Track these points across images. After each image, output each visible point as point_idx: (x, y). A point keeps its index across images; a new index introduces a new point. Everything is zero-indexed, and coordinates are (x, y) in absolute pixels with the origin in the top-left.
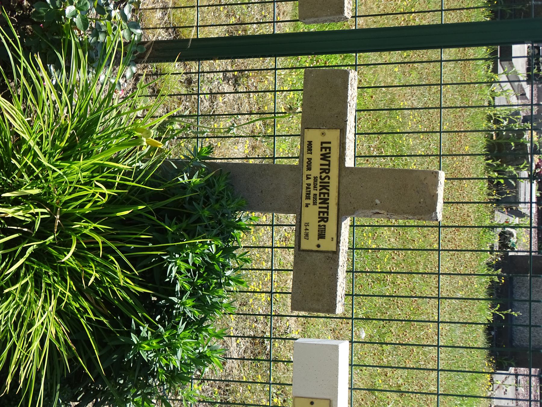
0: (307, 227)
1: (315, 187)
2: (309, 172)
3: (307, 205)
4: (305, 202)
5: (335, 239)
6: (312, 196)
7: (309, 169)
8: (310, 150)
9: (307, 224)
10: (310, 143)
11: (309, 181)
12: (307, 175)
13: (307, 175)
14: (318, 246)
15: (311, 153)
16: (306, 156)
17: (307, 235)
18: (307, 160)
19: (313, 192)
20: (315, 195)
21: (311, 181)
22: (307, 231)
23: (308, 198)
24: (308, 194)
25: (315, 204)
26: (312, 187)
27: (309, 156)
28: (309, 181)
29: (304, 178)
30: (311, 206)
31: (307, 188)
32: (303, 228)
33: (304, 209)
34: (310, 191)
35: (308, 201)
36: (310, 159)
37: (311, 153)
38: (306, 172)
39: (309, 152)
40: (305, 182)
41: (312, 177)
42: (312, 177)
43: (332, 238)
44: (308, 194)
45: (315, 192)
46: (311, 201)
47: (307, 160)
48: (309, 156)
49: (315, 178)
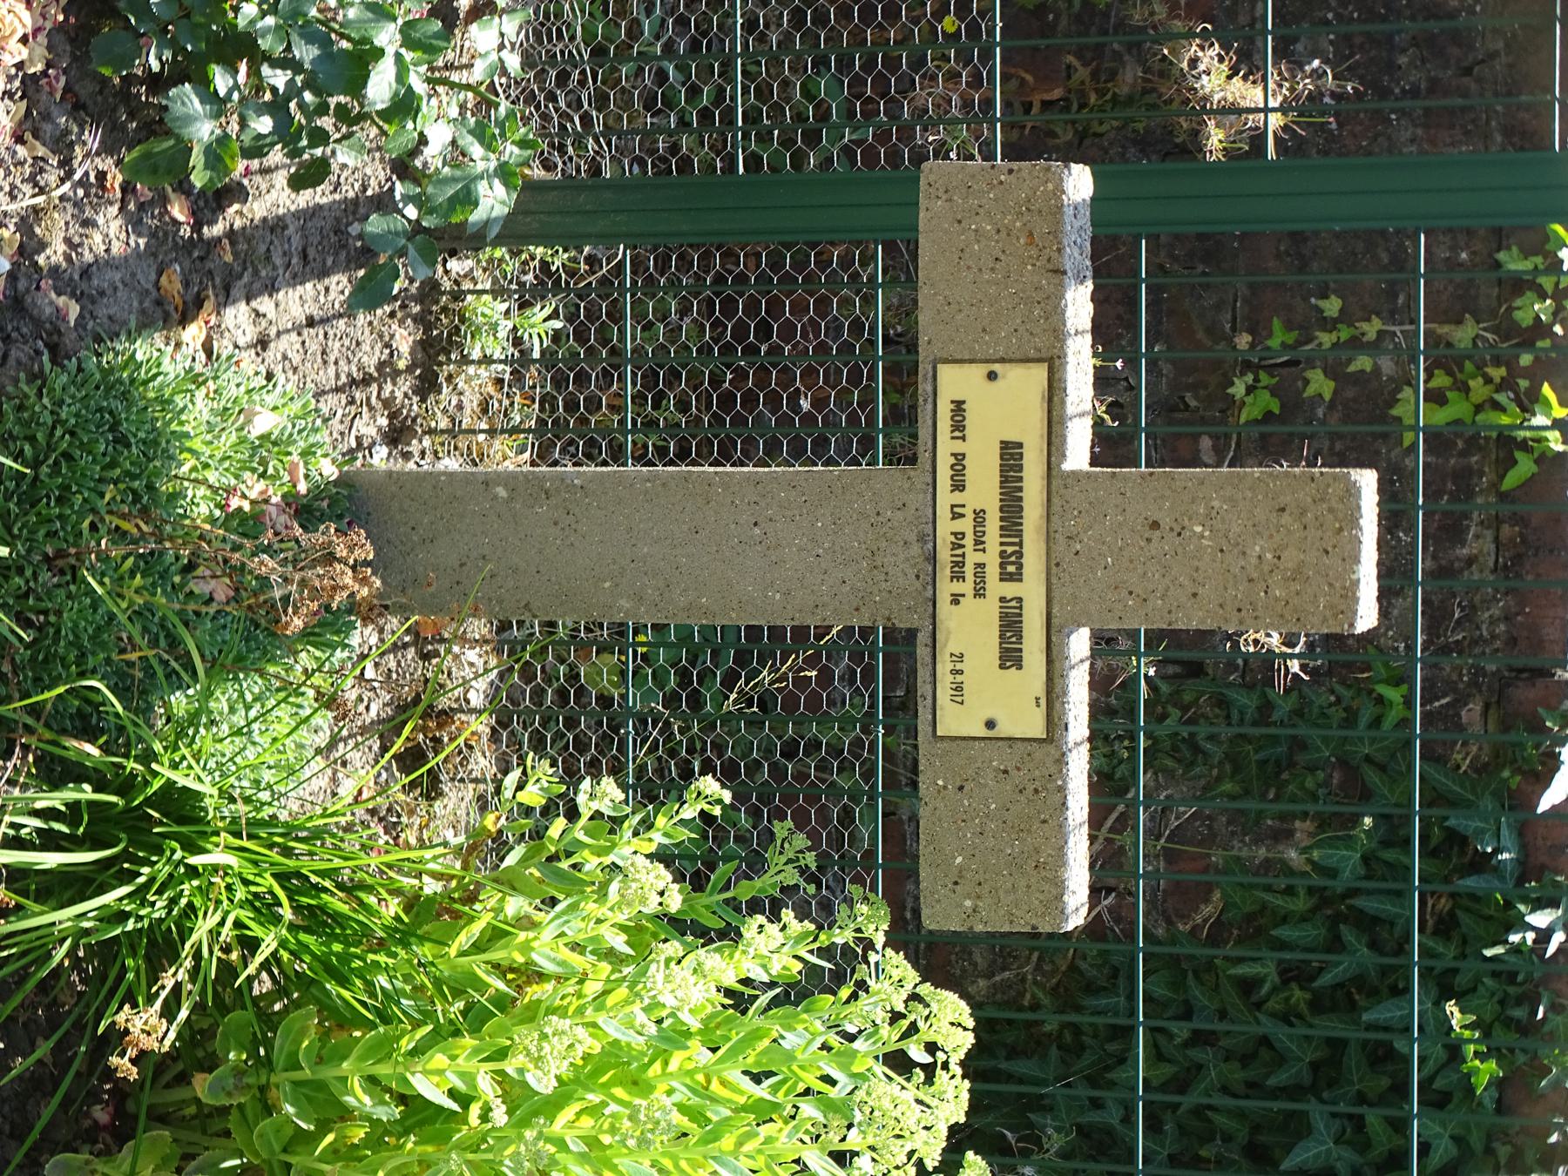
0: (959, 666)
1: (977, 543)
2: (958, 498)
3: (956, 599)
4: (946, 588)
5: (1043, 702)
6: (969, 570)
7: (958, 486)
8: (958, 427)
10: (959, 407)
11: (959, 526)
12: (953, 506)
13: (953, 506)
14: (990, 724)
15: (963, 438)
16: (946, 447)
17: (958, 688)
18: (953, 460)
19: (972, 558)
20: (981, 566)
21: (966, 525)
22: (959, 678)
23: (958, 576)
25: (979, 593)
26: (969, 541)
27: (959, 447)
28: (959, 526)
30: (968, 601)
32: (944, 667)
34: (963, 555)
35: (957, 587)
36: (959, 458)
37: (963, 438)
38: (945, 498)
39: (957, 434)
40: (945, 527)
41: (968, 511)
42: (968, 511)
43: (1037, 699)
44: (959, 564)
45: (979, 557)
46: (967, 587)
47: (953, 460)
48: (959, 447)
49: (979, 516)
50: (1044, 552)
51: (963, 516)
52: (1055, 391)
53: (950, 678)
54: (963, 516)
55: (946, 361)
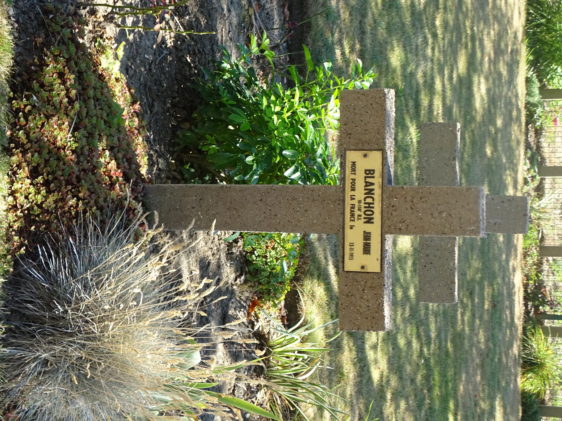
2: (353, 193)
6: (356, 217)
7: (353, 189)
8: (354, 170)
9: (352, 245)
10: (354, 164)
11: (353, 202)
15: (355, 174)
17: (352, 255)
18: (351, 181)
22: (352, 252)
24: (352, 215)
27: (353, 176)
28: (353, 202)
29: (348, 199)
31: (352, 208)
33: (347, 230)
36: (354, 180)
37: (355, 174)
38: (348, 193)
40: (348, 202)
44: (352, 215)
47: (351, 181)
48: (353, 176)
50: (381, 211)
51: (354, 199)
52: (384, 158)
53: (349, 252)
54: (354, 199)
55: (351, 150)
